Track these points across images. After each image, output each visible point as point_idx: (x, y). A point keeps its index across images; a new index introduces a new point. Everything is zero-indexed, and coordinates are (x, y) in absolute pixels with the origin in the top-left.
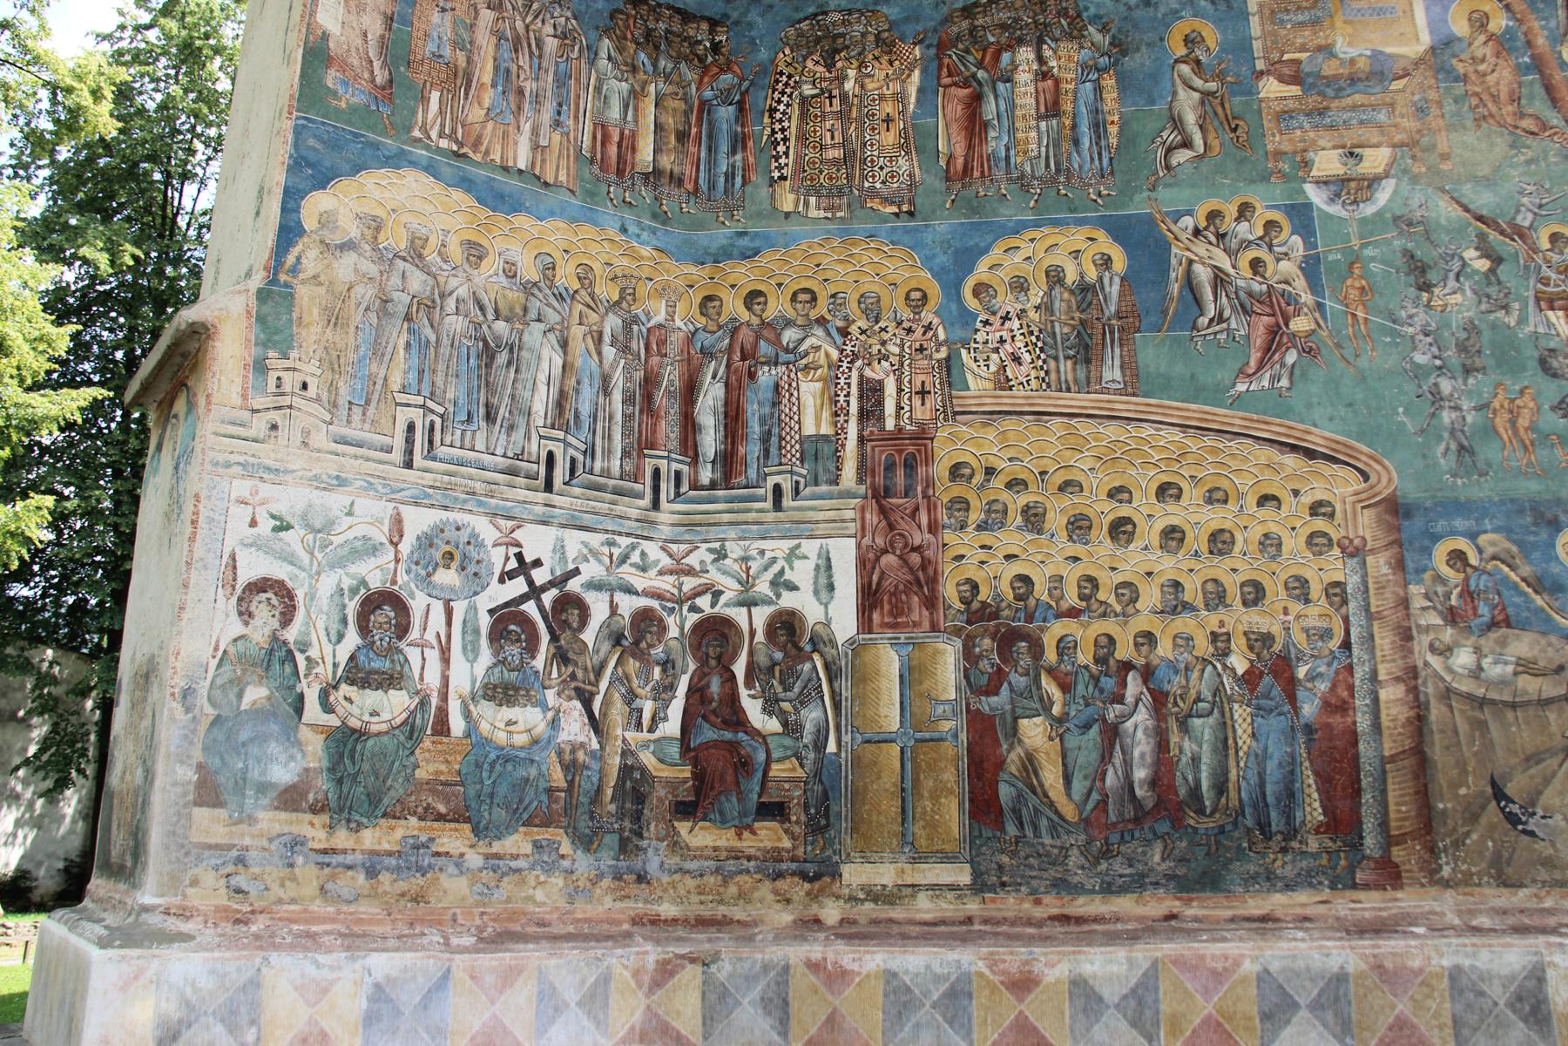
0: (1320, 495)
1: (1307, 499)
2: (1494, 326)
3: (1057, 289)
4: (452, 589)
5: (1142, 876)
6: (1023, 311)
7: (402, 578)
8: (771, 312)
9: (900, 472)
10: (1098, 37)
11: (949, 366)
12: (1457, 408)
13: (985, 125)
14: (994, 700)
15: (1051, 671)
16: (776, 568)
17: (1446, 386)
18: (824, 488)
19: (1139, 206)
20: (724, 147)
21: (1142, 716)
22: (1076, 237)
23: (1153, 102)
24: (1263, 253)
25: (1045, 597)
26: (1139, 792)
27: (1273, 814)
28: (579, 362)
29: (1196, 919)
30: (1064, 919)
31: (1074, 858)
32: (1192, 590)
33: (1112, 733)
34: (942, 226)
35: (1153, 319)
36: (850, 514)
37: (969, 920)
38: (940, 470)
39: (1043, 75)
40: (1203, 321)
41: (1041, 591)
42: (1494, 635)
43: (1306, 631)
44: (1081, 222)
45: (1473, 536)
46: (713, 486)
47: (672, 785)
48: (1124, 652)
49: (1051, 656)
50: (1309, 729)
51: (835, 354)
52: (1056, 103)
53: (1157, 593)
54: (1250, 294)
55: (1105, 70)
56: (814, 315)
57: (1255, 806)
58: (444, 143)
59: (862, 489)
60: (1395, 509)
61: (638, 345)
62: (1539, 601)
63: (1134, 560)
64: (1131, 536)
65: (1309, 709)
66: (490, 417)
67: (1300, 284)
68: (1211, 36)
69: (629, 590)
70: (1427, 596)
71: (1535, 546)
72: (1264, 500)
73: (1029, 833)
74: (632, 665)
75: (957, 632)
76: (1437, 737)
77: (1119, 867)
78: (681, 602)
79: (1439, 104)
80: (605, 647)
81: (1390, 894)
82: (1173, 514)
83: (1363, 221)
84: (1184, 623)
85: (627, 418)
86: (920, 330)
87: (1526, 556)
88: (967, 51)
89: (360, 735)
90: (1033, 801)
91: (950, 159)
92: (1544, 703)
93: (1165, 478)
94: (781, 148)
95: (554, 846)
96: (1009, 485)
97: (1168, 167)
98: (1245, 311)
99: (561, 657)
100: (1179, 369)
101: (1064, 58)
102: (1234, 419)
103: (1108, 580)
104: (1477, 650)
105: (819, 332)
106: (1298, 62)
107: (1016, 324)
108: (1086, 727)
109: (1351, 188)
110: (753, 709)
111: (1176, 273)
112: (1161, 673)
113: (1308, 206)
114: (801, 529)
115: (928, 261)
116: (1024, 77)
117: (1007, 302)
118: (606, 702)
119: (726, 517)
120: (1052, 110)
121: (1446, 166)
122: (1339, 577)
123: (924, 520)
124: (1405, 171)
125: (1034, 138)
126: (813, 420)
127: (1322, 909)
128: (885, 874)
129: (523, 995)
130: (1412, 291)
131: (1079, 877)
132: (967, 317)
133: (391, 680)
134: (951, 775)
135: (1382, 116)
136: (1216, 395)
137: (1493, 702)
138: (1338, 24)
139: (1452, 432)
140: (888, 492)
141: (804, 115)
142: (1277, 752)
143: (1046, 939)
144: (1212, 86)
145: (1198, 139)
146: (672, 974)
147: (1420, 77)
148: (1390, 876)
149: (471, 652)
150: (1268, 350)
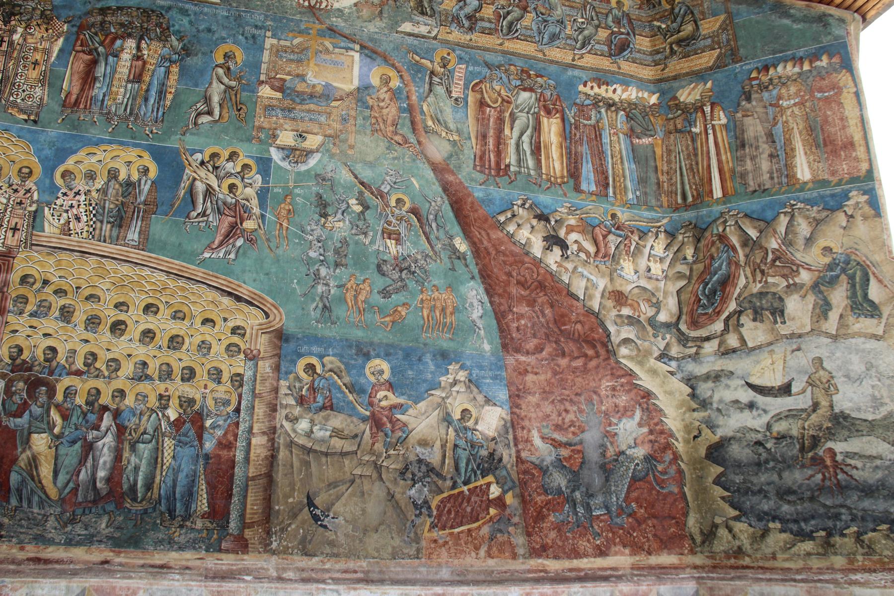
0: (238, 323)
1: (231, 324)
2: (357, 243)
3: (113, 182)
5: (93, 536)
6: (89, 191)
10: (175, 43)
11: (36, 218)
12: (327, 285)
13: (95, 79)
14: (18, 420)
15: (58, 407)
17: (323, 271)
19: (173, 143)
21: (109, 439)
22: (131, 154)
23: (196, 85)
24: (237, 182)
25: (63, 362)
26: (99, 485)
27: (178, 505)
29: (121, 564)
31: (51, 522)
32: (153, 368)
33: (89, 448)
34: (53, 133)
35: (164, 208)
38: (15, 277)
39: (138, 57)
40: (194, 214)
41: (61, 358)
42: (322, 414)
43: (215, 400)
44: (136, 146)
45: (321, 357)
49: (59, 397)
50: (207, 457)
52: (141, 75)
53: (131, 367)
54: (225, 203)
55: (175, 62)
57: (168, 499)
60: (281, 336)
62: (351, 397)
63: (122, 346)
64: (122, 333)
65: (209, 445)
67: (255, 202)
70: (289, 388)
71: (354, 367)
72: (206, 321)
73: (25, 504)
76: (280, 468)
77: (79, 529)
79: (355, 119)
81: (240, 556)
82: (150, 322)
83: (299, 174)
84: (144, 387)
86: (23, 192)
88: (96, 34)
90: (31, 484)
91: (69, 94)
92: (343, 454)
93: (150, 301)
96: (56, 292)
97: (196, 124)
98: (219, 212)
100: (173, 239)
101: (152, 51)
102: (199, 272)
103: (103, 356)
104: (312, 421)
106: (284, 80)
107: (82, 198)
108: (74, 442)
109: (296, 154)
111: (185, 184)
112: (125, 415)
113: (270, 160)
115: (38, 152)
116: (126, 56)
117: (80, 184)
120: (137, 78)
121: (350, 152)
122: (241, 371)
124: (327, 151)
125: (122, 92)
127: (198, 563)
130: (316, 217)
131: (52, 534)
132: (54, 189)
135: (323, 119)
136: (191, 257)
137: (315, 451)
138: (312, 64)
139: (321, 298)
142: (186, 468)
144: (233, 83)
147: (350, 102)
148: (242, 545)
150: (227, 236)
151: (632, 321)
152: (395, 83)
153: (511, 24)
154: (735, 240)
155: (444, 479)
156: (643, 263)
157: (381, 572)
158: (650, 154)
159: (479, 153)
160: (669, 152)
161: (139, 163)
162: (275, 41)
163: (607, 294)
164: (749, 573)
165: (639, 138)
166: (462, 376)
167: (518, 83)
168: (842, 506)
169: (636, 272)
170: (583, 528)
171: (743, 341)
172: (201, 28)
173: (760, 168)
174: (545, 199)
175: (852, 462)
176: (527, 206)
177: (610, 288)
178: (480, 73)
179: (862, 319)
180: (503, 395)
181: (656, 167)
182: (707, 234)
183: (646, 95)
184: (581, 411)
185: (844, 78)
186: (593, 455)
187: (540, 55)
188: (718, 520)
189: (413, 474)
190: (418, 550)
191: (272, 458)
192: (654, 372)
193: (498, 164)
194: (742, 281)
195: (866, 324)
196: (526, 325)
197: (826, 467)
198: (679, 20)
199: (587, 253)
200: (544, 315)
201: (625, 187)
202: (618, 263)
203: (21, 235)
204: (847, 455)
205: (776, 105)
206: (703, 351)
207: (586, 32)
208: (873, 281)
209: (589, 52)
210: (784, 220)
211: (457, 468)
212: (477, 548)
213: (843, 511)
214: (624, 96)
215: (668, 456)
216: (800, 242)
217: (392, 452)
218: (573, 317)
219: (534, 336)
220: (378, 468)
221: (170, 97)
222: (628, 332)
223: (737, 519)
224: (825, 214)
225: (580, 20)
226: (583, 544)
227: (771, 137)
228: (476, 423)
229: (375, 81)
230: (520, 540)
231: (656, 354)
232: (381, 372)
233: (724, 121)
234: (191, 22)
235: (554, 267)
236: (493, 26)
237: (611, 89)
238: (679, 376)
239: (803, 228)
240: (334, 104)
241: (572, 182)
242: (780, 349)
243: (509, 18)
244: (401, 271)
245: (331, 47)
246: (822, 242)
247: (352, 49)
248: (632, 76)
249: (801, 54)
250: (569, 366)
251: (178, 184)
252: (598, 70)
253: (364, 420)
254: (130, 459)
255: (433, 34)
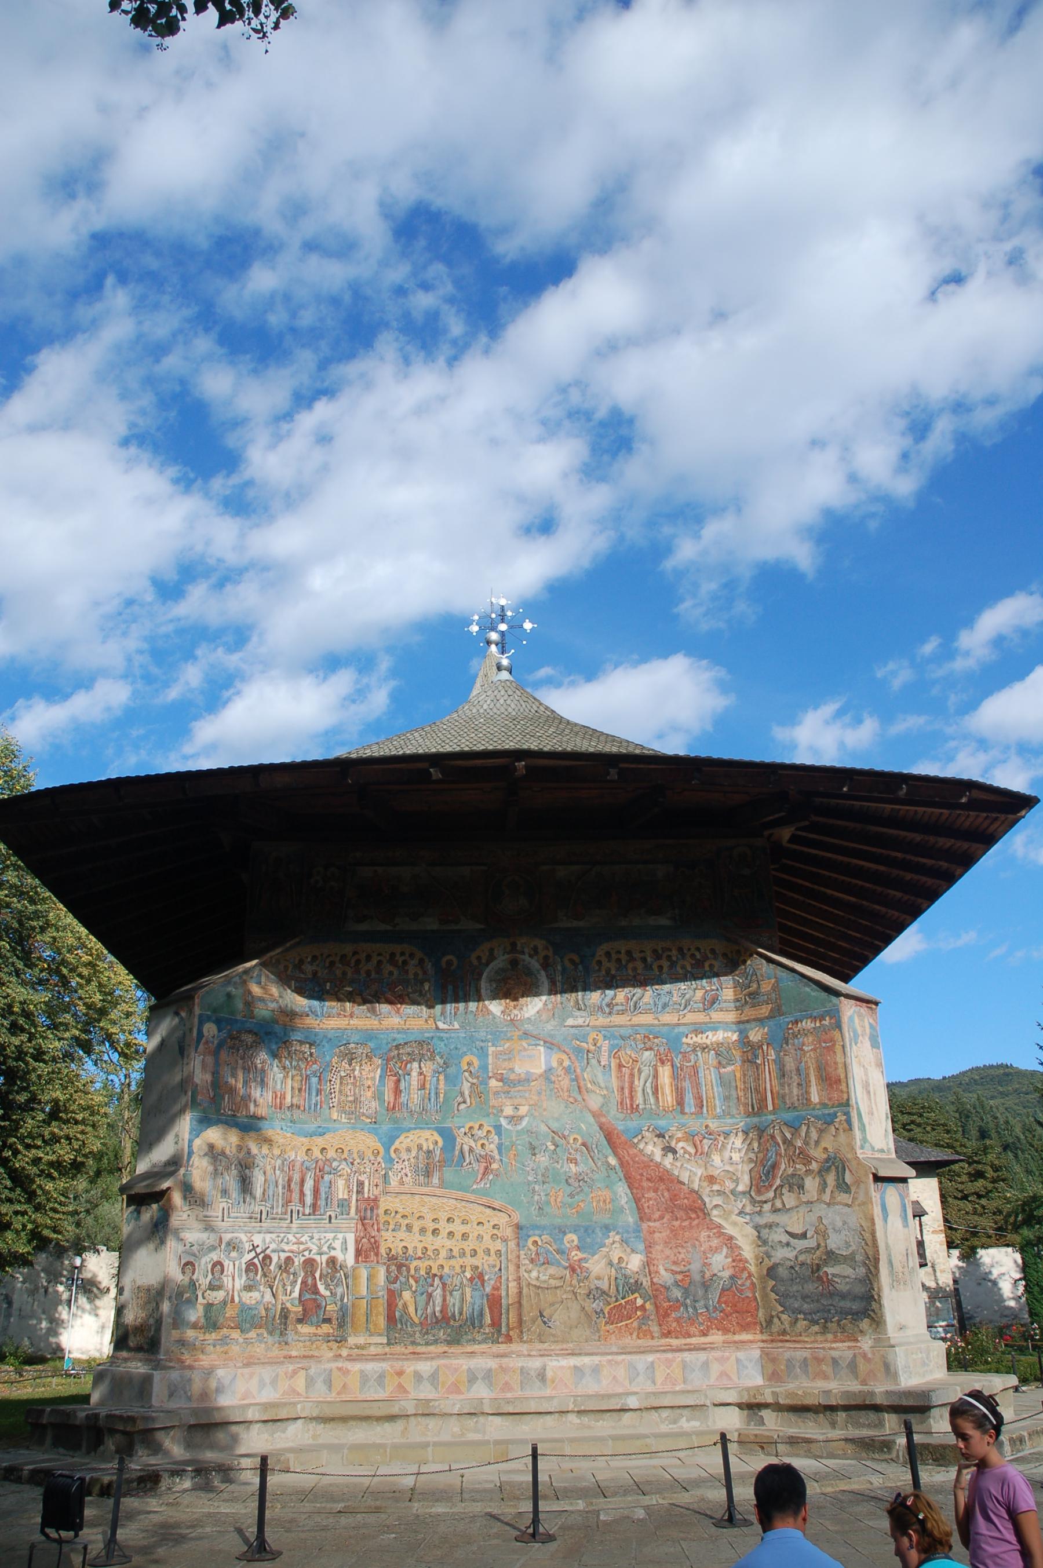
0: (496, 1223)
1: (492, 1224)
2: (554, 1168)
4: (235, 1258)
5: (437, 1340)
7: (222, 1256)
8: (328, 1157)
9: (369, 1211)
10: (439, 1060)
11: (385, 1176)
12: (539, 1195)
13: (401, 1091)
15: (412, 1276)
16: (329, 1242)
17: (537, 1188)
18: (345, 1216)
20: (314, 1094)
21: (439, 1291)
22: (427, 1134)
23: (455, 1086)
24: (485, 1142)
28: (269, 1178)
30: (414, 1353)
31: (418, 1335)
32: (455, 1253)
34: (385, 1127)
36: (353, 1225)
37: (386, 1354)
38: (381, 1211)
39: (421, 1074)
41: (410, 1252)
42: (544, 1267)
44: (429, 1129)
46: (309, 1215)
47: (296, 1313)
48: (434, 1271)
49: (412, 1272)
50: (487, 1295)
51: (349, 1171)
52: (424, 1084)
56: (343, 1157)
58: (230, 1113)
59: (357, 1217)
60: (518, 1227)
61: (286, 1169)
62: (558, 1257)
63: (441, 1242)
66: (244, 1202)
67: (496, 1152)
68: (476, 1062)
69: (284, 1251)
72: (479, 1223)
74: (284, 1275)
75: (385, 1264)
77: (430, 1337)
78: (299, 1253)
80: (277, 1270)
82: (451, 1227)
83: (517, 1131)
84: (453, 1262)
85: (283, 1193)
87: (555, 1243)
89: (212, 1305)
92: (556, 1288)
94: (333, 1095)
95: (262, 1334)
99: (265, 1275)
101: (428, 1067)
102: (472, 1198)
103: (430, 1248)
104: (539, 1271)
105: (344, 1163)
106: (502, 1074)
107: (406, 1163)
108: (423, 1294)
109: (514, 1119)
110: (321, 1288)
111: (458, 1148)
113: (501, 1125)
114: (337, 1230)
115: (380, 1139)
116: (414, 1074)
117: (404, 1155)
118: (277, 1289)
119: (314, 1225)
120: (423, 1087)
121: (544, 1113)
123: (376, 1228)
124: (532, 1115)
126: (341, 1193)
127: (488, 1350)
128: (361, 1340)
129: (255, 1381)
131: (418, 1340)
132: (391, 1160)
133: (219, 1288)
134: (382, 1309)
135: (527, 1095)
140: (365, 1218)
141: (341, 1083)
142: (478, 1302)
143: (407, 1359)
144: (475, 1081)
145: (468, 1101)
146: (296, 1373)
148: (509, 1339)
149: (240, 1276)
151: (719, 1193)
152: (567, 1063)
153: (636, 1003)
154: (779, 1139)
155: (611, 1297)
156: (727, 1154)
157: (580, 1349)
158: (733, 1077)
159: (619, 1100)
160: (745, 1075)
161: (431, 1139)
162: (493, 1049)
163: (703, 1179)
164: (787, 1345)
165: (724, 1068)
166: (617, 1238)
167: (643, 1046)
168: (831, 1305)
169: (722, 1161)
170: (692, 1321)
171: (784, 1205)
172: (452, 1047)
173: (792, 1092)
174: (662, 1123)
175: (836, 1279)
176: (651, 1130)
177: (705, 1174)
178: (617, 1045)
179: (842, 1194)
180: (641, 1247)
181: (737, 1086)
182: (765, 1134)
183: (730, 1034)
184: (688, 1252)
185: (836, 1034)
186: (697, 1277)
187: (656, 1022)
188: (774, 1313)
189: (594, 1296)
190: (599, 1337)
191: (520, 1293)
192: (735, 1224)
193: (632, 1105)
194: (783, 1166)
195: (843, 1197)
196: (653, 1204)
197: (824, 1282)
198: (749, 978)
199: (690, 1154)
200: (664, 1197)
201: (715, 1105)
202: (710, 1157)
203: (381, 1188)
204: (834, 1275)
205: (802, 1050)
206: (763, 1210)
207: (687, 996)
208: (847, 1171)
209: (689, 1012)
210: (804, 1128)
211: (617, 1290)
212: (631, 1334)
213: (832, 1308)
214: (714, 1040)
215: (745, 1275)
216: (812, 1143)
217: (582, 1284)
218: (682, 1195)
219: (659, 1210)
220: (575, 1294)
221: (442, 1096)
222: (718, 1200)
223: (782, 1312)
224: (825, 1126)
225: (683, 987)
226: (693, 1330)
227: (798, 1070)
228: (627, 1264)
229: (555, 1064)
230: (655, 1329)
231: (737, 1212)
232: (573, 1241)
233: (774, 1057)
234: (445, 1045)
235: (669, 1166)
236: (624, 1008)
237: (704, 1036)
238: (751, 1225)
239: (814, 1135)
240: (533, 1084)
241: (679, 1108)
242: (803, 1209)
243: (634, 998)
244: (579, 1181)
245: (526, 1045)
246: (823, 1144)
247: (539, 1045)
248: (720, 1022)
249: (815, 1014)
250: (680, 1226)
251: (454, 1148)
252: (695, 1023)
253: (566, 1268)
254: (450, 1301)
255: (586, 1024)
